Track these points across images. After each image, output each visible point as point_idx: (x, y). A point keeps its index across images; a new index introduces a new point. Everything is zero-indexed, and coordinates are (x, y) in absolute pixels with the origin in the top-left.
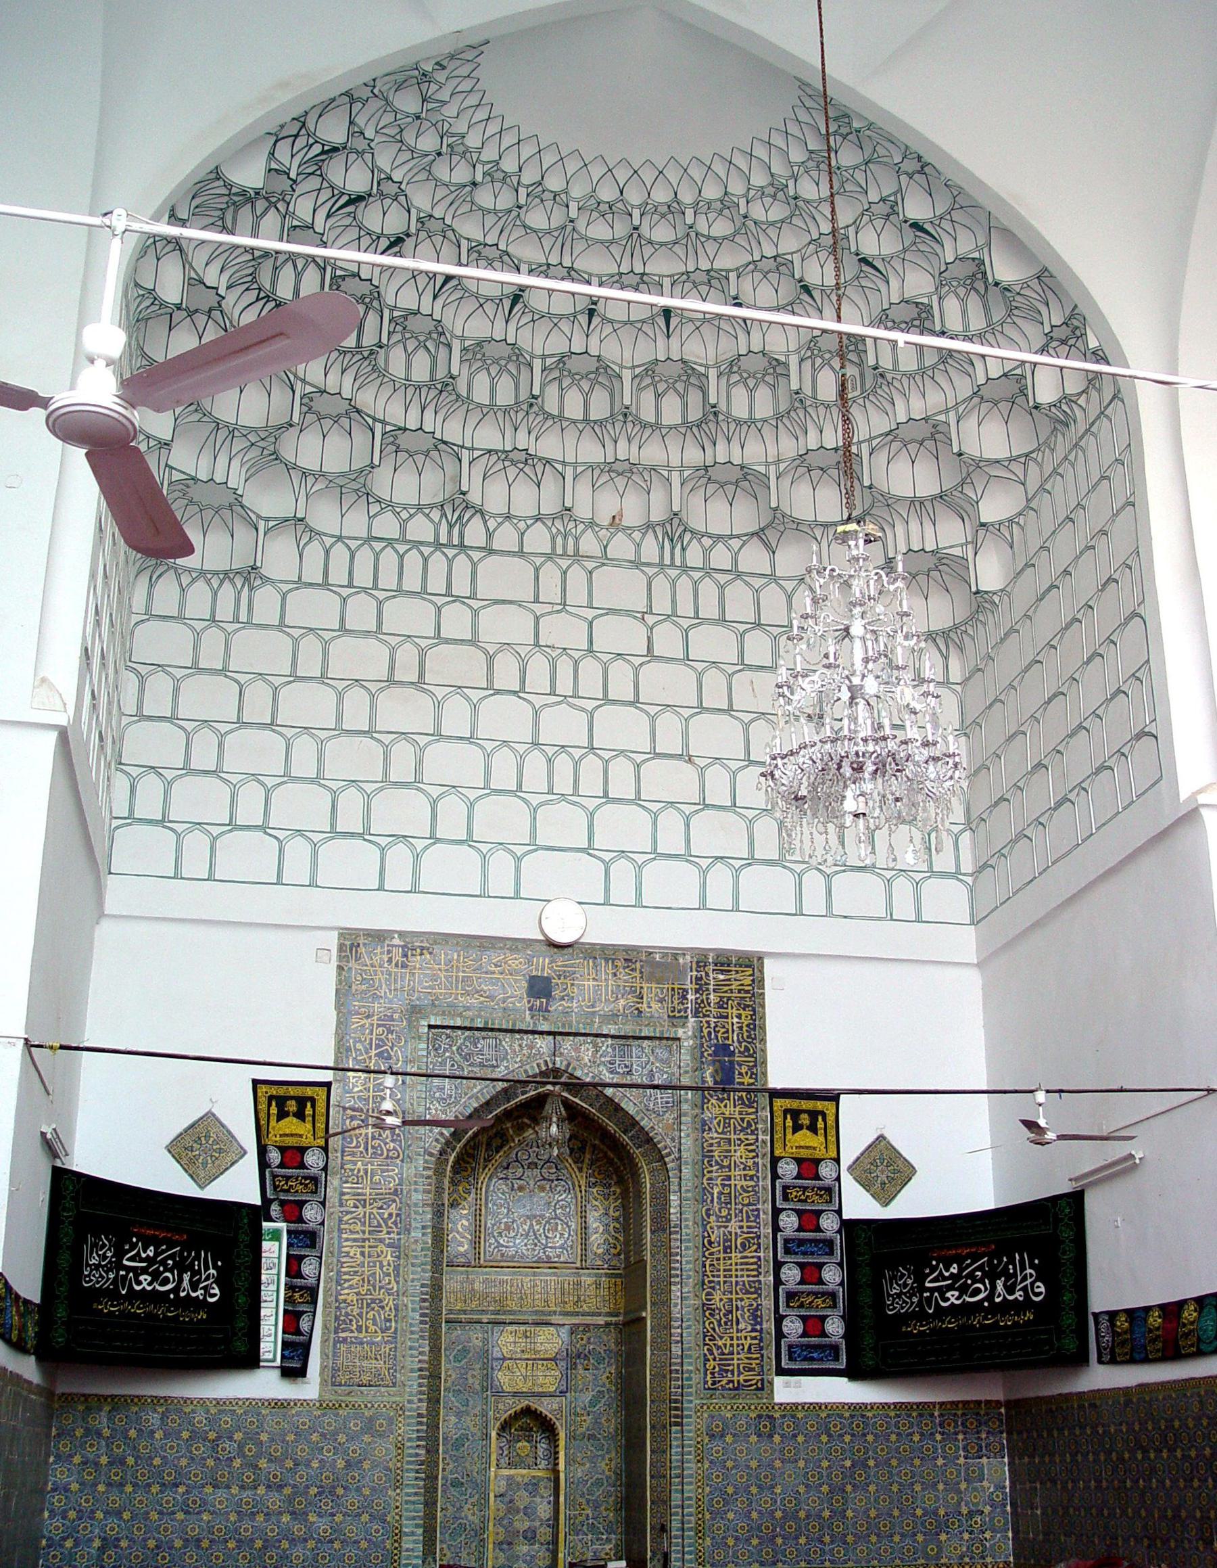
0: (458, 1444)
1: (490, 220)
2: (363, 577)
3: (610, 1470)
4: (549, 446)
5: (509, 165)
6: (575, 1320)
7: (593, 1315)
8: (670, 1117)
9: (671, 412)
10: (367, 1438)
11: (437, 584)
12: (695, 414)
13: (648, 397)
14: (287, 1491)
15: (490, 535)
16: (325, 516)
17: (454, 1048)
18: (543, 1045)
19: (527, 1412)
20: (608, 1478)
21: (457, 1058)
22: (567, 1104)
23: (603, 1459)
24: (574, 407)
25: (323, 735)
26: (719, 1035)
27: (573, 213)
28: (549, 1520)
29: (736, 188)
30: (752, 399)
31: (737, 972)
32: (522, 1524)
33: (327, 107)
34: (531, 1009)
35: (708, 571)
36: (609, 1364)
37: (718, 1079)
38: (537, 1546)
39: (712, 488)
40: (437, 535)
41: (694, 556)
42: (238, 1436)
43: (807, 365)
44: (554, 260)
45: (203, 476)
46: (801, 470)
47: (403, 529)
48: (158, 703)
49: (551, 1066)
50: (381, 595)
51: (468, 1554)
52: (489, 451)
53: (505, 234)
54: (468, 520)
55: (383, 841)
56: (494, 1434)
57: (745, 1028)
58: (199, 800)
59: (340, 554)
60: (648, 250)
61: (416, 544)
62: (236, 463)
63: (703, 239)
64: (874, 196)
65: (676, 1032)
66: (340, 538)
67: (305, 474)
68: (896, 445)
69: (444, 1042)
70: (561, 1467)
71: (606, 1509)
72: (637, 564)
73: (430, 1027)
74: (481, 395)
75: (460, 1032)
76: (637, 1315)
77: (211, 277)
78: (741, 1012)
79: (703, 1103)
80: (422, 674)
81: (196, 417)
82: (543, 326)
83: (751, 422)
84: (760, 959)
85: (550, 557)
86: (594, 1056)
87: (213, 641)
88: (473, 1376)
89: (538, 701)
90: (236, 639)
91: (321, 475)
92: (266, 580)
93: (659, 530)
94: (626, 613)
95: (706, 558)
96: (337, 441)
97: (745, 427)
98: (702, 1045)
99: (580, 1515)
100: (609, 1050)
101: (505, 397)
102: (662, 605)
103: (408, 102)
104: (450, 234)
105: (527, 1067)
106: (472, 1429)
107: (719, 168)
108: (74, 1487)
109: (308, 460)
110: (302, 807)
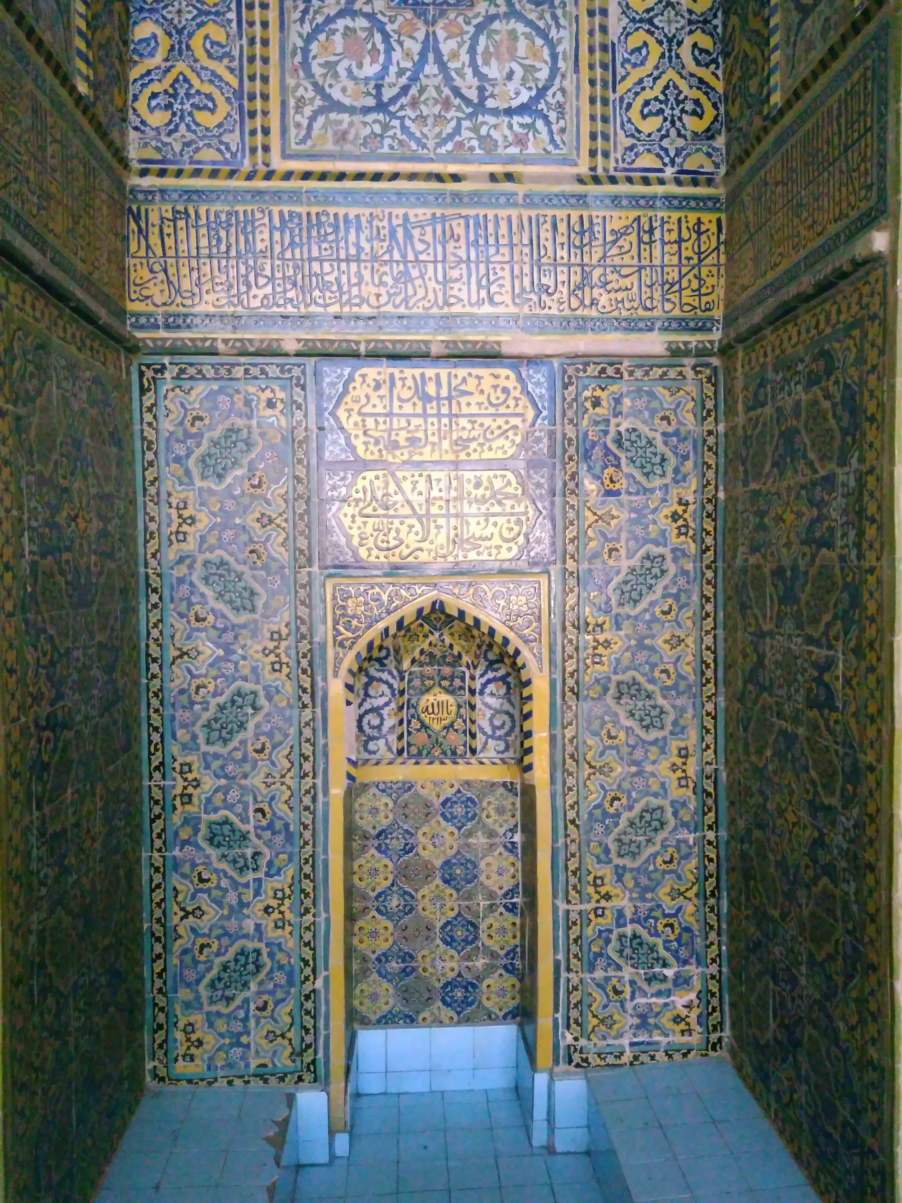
3: (683, 781)
6: (582, 343)
7: (631, 325)
19: (437, 616)
20: (678, 806)
23: (663, 751)
28: (511, 893)
32: (436, 904)
36: (679, 478)
38: (480, 963)
51: (271, 1036)
56: (336, 688)
70: (540, 775)
71: (676, 894)
76: (841, 259)
88: (266, 521)
99: (599, 912)
106: (267, 676)
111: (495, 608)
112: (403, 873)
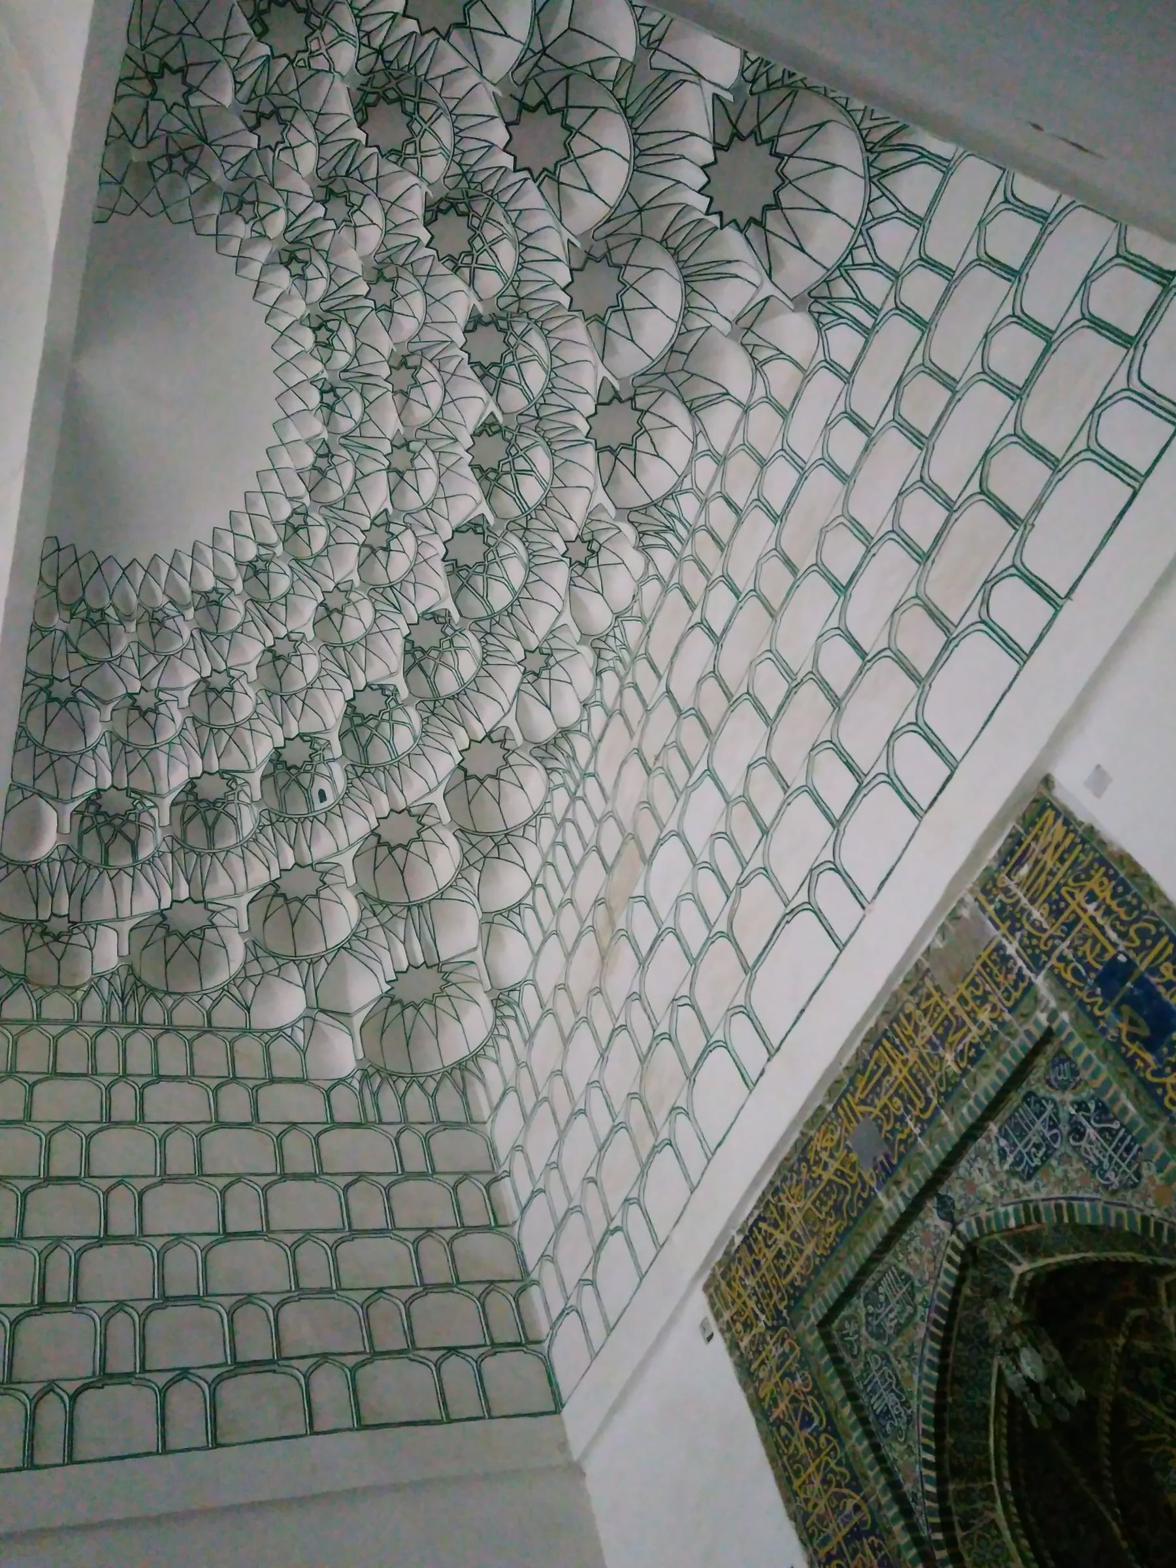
1: (302, 589)
15: (587, 736)
16: (510, 884)
17: (863, 1331)
18: (932, 1219)
21: (874, 1344)
26: (1090, 958)
31: (1036, 838)
34: (879, 1188)
37: (1145, 1032)
39: (643, 443)
44: (361, 538)
45: (386, 987)
49: (961, 1246)
52: (518, 690)
53: (318, 576)
54: (572, 747)
57: (1114, 904)
63: (355, 363)
65: (1037, 1023)
66: (534, 885)
68: (565, 175)
73: (824, 1324)
75: (855, 1300)
78: (1089, 885)
79: (1159, 1100)
81: (323, 965)
84: (1047, 781)
86: (993, 1174)
91: (460, 870)
93: (648, 540)
97: (559, 383)
98: (1081, 1003)
100: (1003, 1142)
103: (126, 639)
104: (294, 636)
105: (943, 1278)
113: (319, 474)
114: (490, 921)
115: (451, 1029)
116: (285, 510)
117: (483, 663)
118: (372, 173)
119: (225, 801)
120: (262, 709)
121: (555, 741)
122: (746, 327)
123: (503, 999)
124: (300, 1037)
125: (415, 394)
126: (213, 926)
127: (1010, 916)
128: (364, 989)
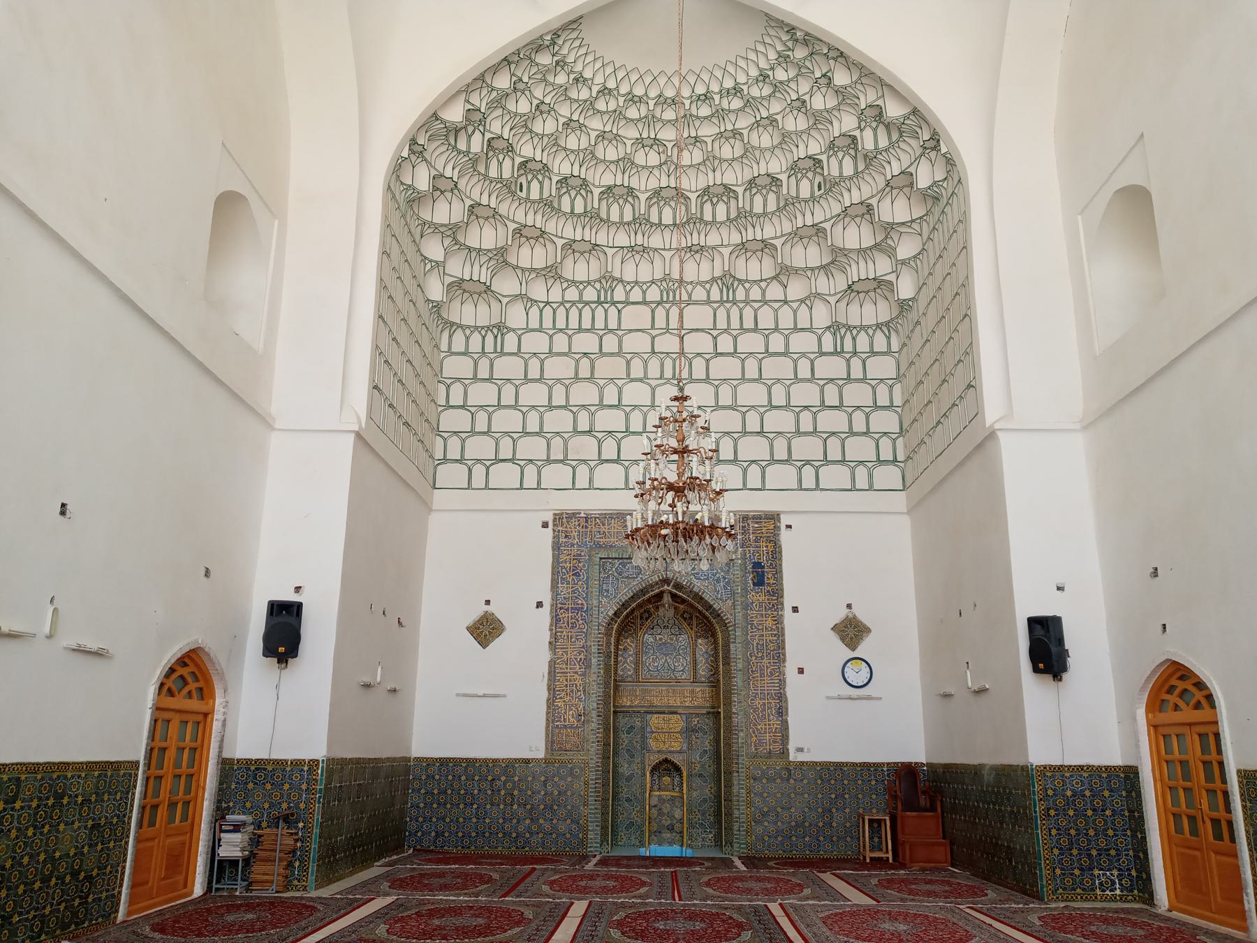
0: (629, 779)
1: (606, 117)
2: (561, 324)
4: (656, 241)
5: (611, 84)
8: (730, 602)
9: (721, 215)
10: (569, 779)
11: (600, 324)
12: (733, 215)
13: (708, 207)
14: (528, 807)
15: (627, 293)
16: (538, 291)
19: (666, 761)
22: (674, 596)
24: (667, 218)
25: (542, 409)
27: (651, 108)
29: (742, 78)
30: (765, 201)
33: (495, 69)
35: (747, 302)
39: (749, 254)
40: (599, 297)
41: (740, 294)
42: (503, 778)
43: (793, 179)
44: (645, 135)
46: (796, 239)
47: (581, 295)
48: (456, 399)
50: (570, 332)
55: (574, 463)
58: (480, 447)
59: (548, 311)
60: (697, 123)
61: (587, 303)
62: (484, 269)
64: (818, 74)
67: (523, 270)
69: (608, 566)
72: (708, 302)
74: (615, 217)
77: (448, 173)
80: (592, 373)
82: (645, 174)
83: (765, 214)
85: (659, 303)
87: (484, 364)
89: (653, 383)
90: (496, 362)
91: (532, 270)
92: (510, 330)
94: (702, 330)
95: (747, 295)
96: (539, 250)
101: (628, 217)
102: (722, 324)
103: (545, 59)
107: (731, 69)
108: (422, 805)
109: (525, 263)
110: (532, 448)
111: (676, 759)
112: (659, 814)
113: (661, 100)
114: (520, 296)
115: (456, 304)
116: (639, 91)
117: (622, 223)
118: (820, 126)
119: (494, 149)
120: (546, 139)
121: (614, 279)
122: (818, 295)
123: (500, 328)
124: (428, 267)
125: (723, 140)
126: (442, 192)
127: (745, 531)
128: (457, 268)
